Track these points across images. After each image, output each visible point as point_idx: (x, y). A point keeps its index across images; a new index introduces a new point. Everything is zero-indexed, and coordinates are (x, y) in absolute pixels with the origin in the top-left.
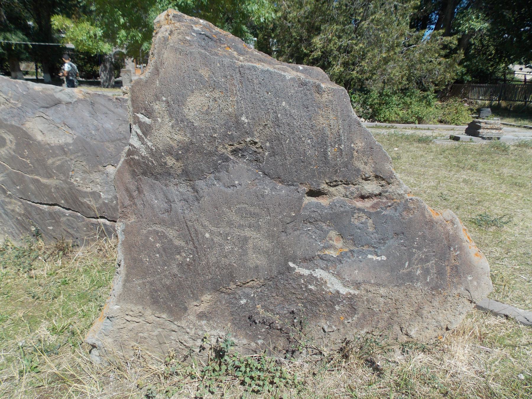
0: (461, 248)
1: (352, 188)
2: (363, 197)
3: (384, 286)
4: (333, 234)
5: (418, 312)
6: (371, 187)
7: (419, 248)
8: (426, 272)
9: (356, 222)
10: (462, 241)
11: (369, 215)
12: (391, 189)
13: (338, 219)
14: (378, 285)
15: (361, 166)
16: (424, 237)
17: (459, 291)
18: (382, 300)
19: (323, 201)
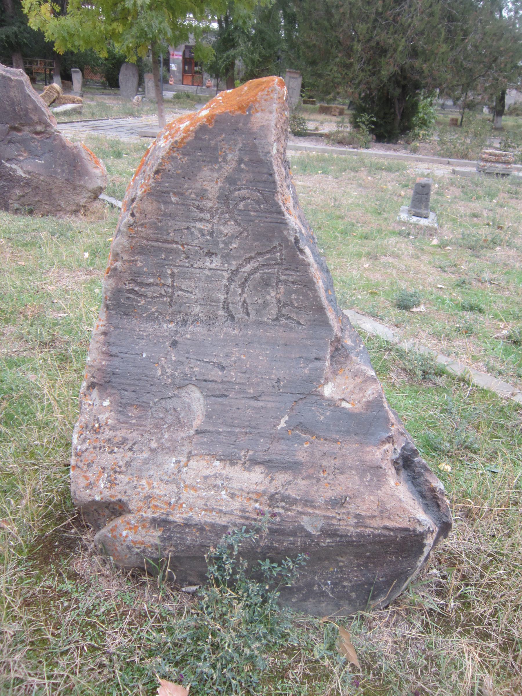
0: (81, 161)
1: (32, 128)
2: (37, 133)
4: (23, 149)
5: (60, 193)
6: (39, 128)
7: (59, 159)
8: (63, 171)
9: (33, 144)
10: (82, 158)
11: (39, 141)
12: (49, 129)
13: (23, 142)
15: (33, 117)
16: (61, 153)
19: (19, 134)
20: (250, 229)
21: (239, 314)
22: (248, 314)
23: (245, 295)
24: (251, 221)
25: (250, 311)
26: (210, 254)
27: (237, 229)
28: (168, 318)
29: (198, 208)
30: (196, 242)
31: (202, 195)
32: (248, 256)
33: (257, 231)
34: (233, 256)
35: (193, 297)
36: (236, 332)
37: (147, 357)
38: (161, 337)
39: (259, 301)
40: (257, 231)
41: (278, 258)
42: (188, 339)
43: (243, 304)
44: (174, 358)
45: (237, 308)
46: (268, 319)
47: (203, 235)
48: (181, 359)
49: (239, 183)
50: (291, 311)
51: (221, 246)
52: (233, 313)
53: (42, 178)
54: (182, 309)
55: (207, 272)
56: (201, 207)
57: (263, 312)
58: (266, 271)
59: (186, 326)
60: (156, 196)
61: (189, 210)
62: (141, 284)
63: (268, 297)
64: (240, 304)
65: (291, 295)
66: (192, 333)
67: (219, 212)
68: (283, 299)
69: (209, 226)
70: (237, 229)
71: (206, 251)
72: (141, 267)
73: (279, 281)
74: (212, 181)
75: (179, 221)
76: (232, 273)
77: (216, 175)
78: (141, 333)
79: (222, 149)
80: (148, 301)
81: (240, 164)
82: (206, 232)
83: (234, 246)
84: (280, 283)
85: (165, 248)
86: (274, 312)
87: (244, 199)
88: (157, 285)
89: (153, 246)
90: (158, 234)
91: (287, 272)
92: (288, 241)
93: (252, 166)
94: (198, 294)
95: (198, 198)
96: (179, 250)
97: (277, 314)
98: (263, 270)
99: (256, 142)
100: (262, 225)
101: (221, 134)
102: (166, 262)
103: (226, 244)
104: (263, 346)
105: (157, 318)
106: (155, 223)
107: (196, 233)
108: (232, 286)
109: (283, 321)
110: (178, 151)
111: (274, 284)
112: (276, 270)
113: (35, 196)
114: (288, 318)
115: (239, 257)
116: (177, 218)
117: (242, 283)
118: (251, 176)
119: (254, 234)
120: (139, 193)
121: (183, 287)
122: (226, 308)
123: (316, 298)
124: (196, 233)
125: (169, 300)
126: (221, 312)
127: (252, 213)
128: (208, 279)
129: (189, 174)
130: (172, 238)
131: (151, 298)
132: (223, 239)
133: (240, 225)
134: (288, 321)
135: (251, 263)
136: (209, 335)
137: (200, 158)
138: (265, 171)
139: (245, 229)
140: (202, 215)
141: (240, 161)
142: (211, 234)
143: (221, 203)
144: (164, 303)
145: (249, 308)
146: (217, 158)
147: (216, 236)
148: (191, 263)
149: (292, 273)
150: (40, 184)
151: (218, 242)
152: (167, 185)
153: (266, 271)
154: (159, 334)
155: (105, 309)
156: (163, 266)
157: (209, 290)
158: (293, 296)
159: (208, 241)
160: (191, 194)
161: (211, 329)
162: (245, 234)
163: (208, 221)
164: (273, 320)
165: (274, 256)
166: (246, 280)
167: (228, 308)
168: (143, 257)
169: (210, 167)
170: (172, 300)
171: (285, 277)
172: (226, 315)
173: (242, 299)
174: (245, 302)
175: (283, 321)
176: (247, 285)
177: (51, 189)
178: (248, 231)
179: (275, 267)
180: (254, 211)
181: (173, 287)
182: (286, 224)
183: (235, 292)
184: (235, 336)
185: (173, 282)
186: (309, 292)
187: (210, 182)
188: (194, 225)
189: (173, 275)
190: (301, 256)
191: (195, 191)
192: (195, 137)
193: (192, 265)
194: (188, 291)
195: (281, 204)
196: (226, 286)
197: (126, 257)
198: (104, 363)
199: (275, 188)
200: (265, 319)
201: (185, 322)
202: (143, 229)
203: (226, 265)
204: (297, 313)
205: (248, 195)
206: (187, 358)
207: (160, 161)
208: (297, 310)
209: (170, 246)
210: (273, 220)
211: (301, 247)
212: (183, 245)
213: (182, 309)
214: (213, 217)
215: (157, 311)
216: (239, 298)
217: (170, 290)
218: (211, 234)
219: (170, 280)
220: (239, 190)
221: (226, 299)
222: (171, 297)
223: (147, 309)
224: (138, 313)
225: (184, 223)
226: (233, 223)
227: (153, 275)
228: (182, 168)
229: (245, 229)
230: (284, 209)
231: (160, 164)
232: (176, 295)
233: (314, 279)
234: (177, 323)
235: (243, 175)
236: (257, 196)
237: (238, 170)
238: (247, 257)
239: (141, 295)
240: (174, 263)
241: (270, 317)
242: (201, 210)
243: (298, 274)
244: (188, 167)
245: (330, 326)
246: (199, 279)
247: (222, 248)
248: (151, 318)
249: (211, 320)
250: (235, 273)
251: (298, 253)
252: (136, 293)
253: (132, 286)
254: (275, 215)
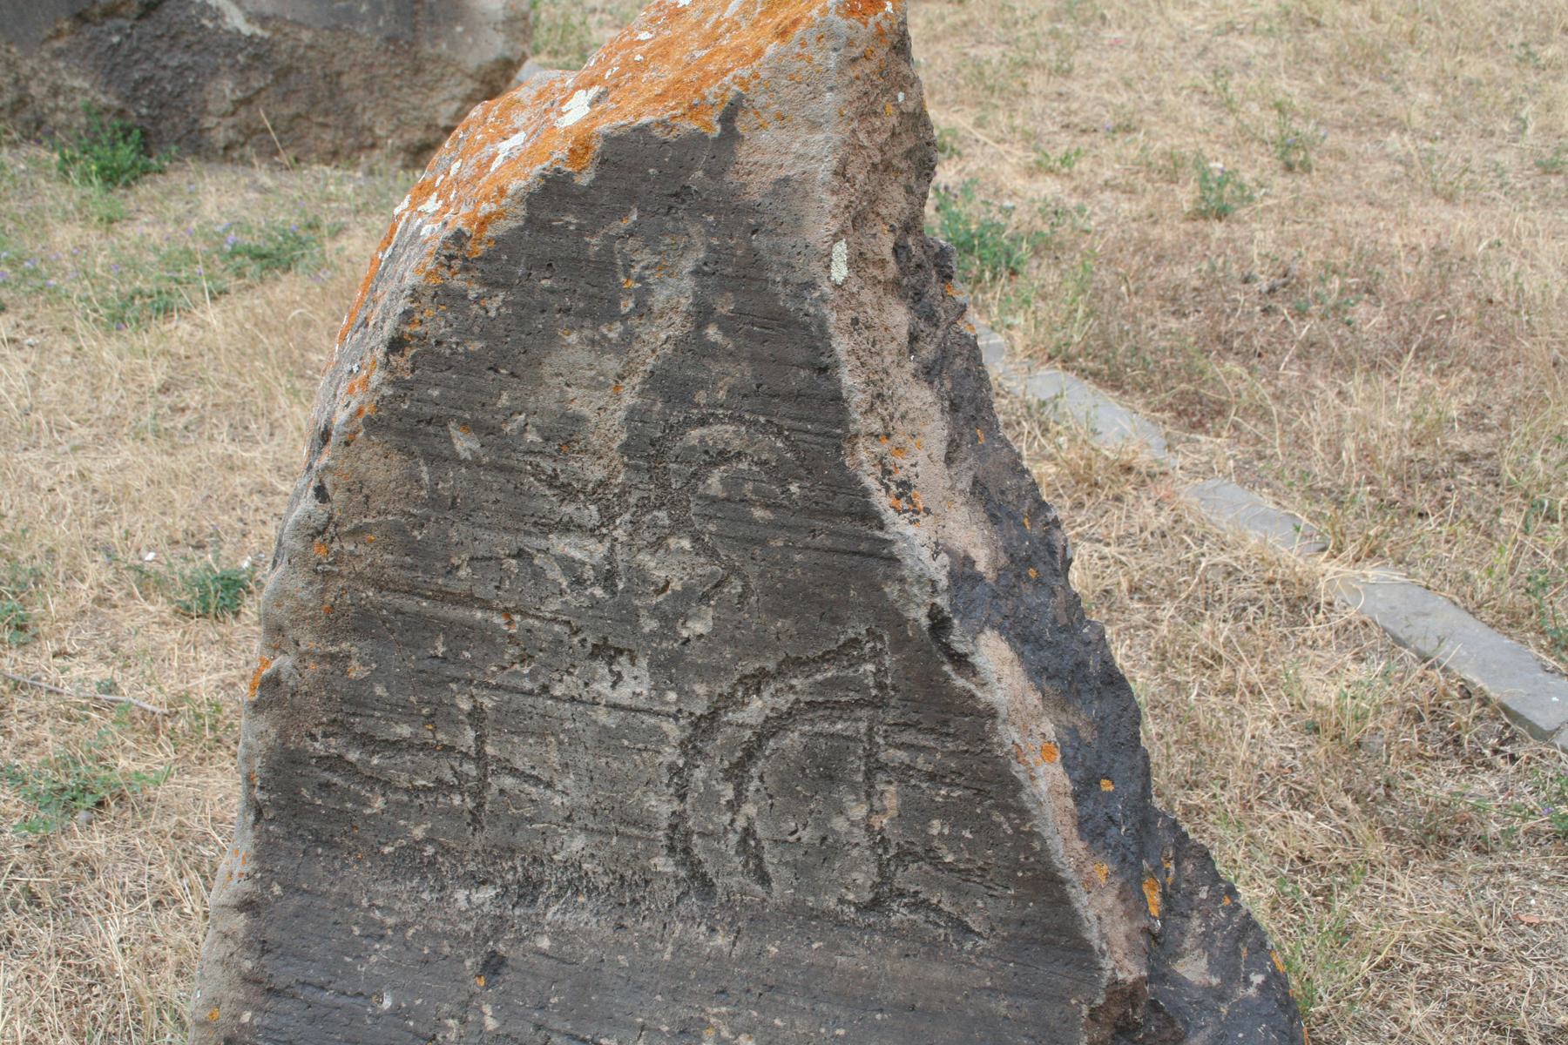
3: (308, 28)
14: (300, 24)
17: (437, 51)
18: (311, 54)
20: (752, 570)
21: (732, 877)
22: (764, 879)
23: (749, 809)
24: (753, 541)
25: (770, 869)
26: (605, 651)
27: (706, 568)
28: (471, 867)
29: (551, 481)
30: (554, 605)
31: (565, 433)
32: (751, 667)
33: (780, 579)
34: (693, 664)
35: (557, 800)
36: (720, 940)
37: (396, 1011)
38: (445, 935)
39: (806, 835)
40: (780, 579)
41: (870, 681)
42: (545, 954)
43: (743, 841)
44: (491, 1024)
45: (721, 854)
46: (841, 901)
47: (579, 582)
48: (512, 1028)
49: (701, 397)
50: (932, 883)
52: (708, 868)
53: (306, 36)
54: (520, 838)
55: (602, 717)
56: (562, 478)
57: (822, 874)
58: (825, 726)
59: (534, 901)
60: (400, 433)
61: (518, 491)
62: (367, 741)
63: (839, 824)
64: (733, 839)
65: (926, 823)
66: (558, 933)
67: (632, 500)
68: (895, 836)
69: (600, 550)
71: (591, 640)
72: (363, 681)
73: (875, 767)
74: (601, 386)
75: (489, 528)
76: (695, 725)
77: (612, 364)
78: (377, 914)
79: (628, 266)
80: (398, 803)
81: (700, 326)
82: (589, 574)
83: (698, 627)
84: (881, 776)
85: (444, 620)
86: (864, 877)
87: (723, 457)
88: (424, 746)
89: (398, 612)
90: (413, 568)
91: (908, 737)
92: (900, 622)
93: (749, 335)
94: (574, 793)
95: (552, 447)
96: (496, 628)
97: (874, 885)
98: (812, 722)
99: (761, 242)
100: (798, 557)
101: (623, 213)
102: (451, 671)
103: (669, 620)
104: (824, 1007)
105: (432, 862)
106: (400, 529)
107: (555, 573)
108: (700, 774)
109: (900, 914)
110: (466, 269)
111: (859, 778)
112: (863, 726)
113: (285, 98)
114: (918, 905)
115: (717, 671)
116: (479, 517)
117: (732, 766)
118: (741, 373)
119: (769, 591)
120: (341, 416)
121: (520, 763)
122: (678, 844)
123: (1026, 839)
124: (555, 573)
125: (470, 804)
126: (663, 864)
127: (758, 513)
128: (607, 740)
129: (514, 353)
130: (465, 586)
131: (407, 790)
132: (655, 600)
133: (713, 554)
134: (918, 917)
135: (766, 695)
136: (621, 947)
137: (551, 298)
138: (800, 354)
139: (734, 570)
140: (569, 509)
141: (702, 314)
142: (608, 578)
143: (637, 468)
144: (452, 813)
145: (767, 857)
146: (615, 303)
147: (626, 591)
148: (542, 680)
149: (922, 740)
150: (302, 58)
151: (635, 613)
152: (436, 393)
153: (825, 726)
154: (439, 926)
155: (251, 818)
156: (443, 683)
157: (613, 782)
158: (936, 827)
159: (595, 604)
160: (523, 430)
161: (628, 922)
162: (735, 587)
164: (863, 909)
165: (851, 673)
166: (750, 755)
167: (687, 851)
168: (367, 646)
169: (587, 332)
170: (480, 806)
171: (902, 755)
172: (682, 874)
173: (741, 823)
174: (748, 832)
175: (900, 914)
176: (754, 771)
177: (339, 74)
178: (744, 578)
179: (860, 713)
180: (766, 506)
181: (480, 758)
182: (893, 560)
183: (710, 797)
184: (718, 957)
185: (481, 740)
186: (998, 817)
187: (594, 389)
188: (543, 544)
189: (476, 716)
190: (960, 682)
191: (538, 420)
192: (528, 221)
193: (545, 689)
194: (537, 781)
195: (871, 482)
196: (674, 770)
197: (308, 642)
198: (246, 1017)
199: (842, 419)
200: (831, 902)
201: (529, 890)
202: (361, 549)
203: (672, 696)
204: (954, 889)
205: (736, 444)
206: (538, 1027)
207: (402, 305)
208: (954, 878)
209: (460, 613)
210: (842, 544)
211: (961, 648)
212: (506, 612)
213: (520, 838)
214: (612, 518)
215: (429, 840)
216: (727, 818)
217: (470, 769)
218: (608, 578)
219: (470, 734)
220: (703, 422)
221: (679, 816)
222: (478, 794)
223: (392, 832)
224: (365, 843)
225: (507, 537)
226: (686, 544)
227: (409, 714)
228: (484, 334)
229: (734, 570)
230: (882, 501)
231: (407, 315)
232: (494, 789)
233: (1017, 770)
234: (505, 887)
235: (716, 368)
236: (772, 449)
237: (693, 348)
238: (749, 670)
239: (371, 780)
240: (479, 675)
241: (851, 897)
242: (567, 492)
243: (950, 746)
244: (508, 332)
245: (1087, 948)
246: (575, 740)
247: (653, 633)
248: (411, 863)
249: (627, 891)
250: (706, 725)
251: (947, 668)
252: (351, 769)
253: (335, 745)
254: (846, 525)
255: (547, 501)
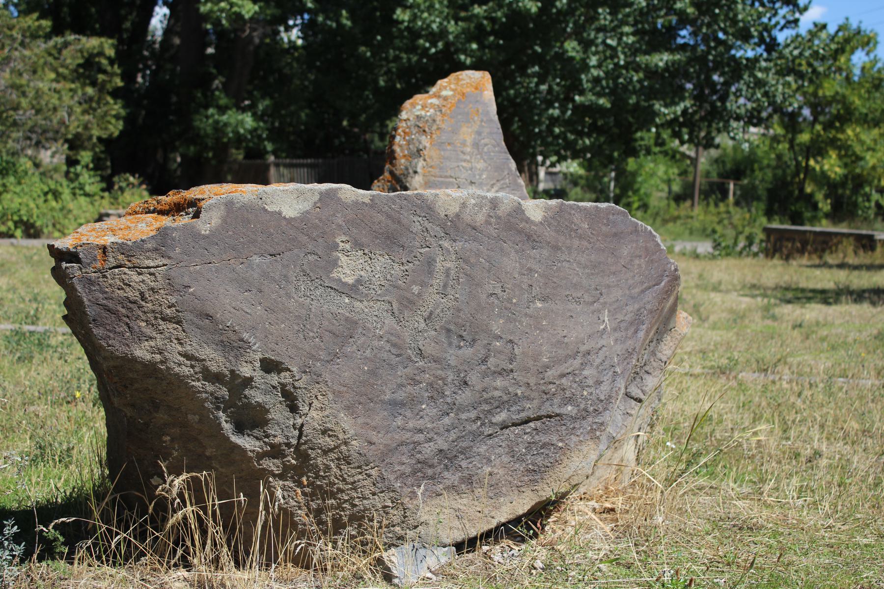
27: (485, 165)
31: (464, 144)
51: (477, 177)
70: (485, 165)
103: (480, 175)
129: (455, 131)
163: (468, 161)
209: (448, 180)
218: (471, 169)
255: (462, 156)
